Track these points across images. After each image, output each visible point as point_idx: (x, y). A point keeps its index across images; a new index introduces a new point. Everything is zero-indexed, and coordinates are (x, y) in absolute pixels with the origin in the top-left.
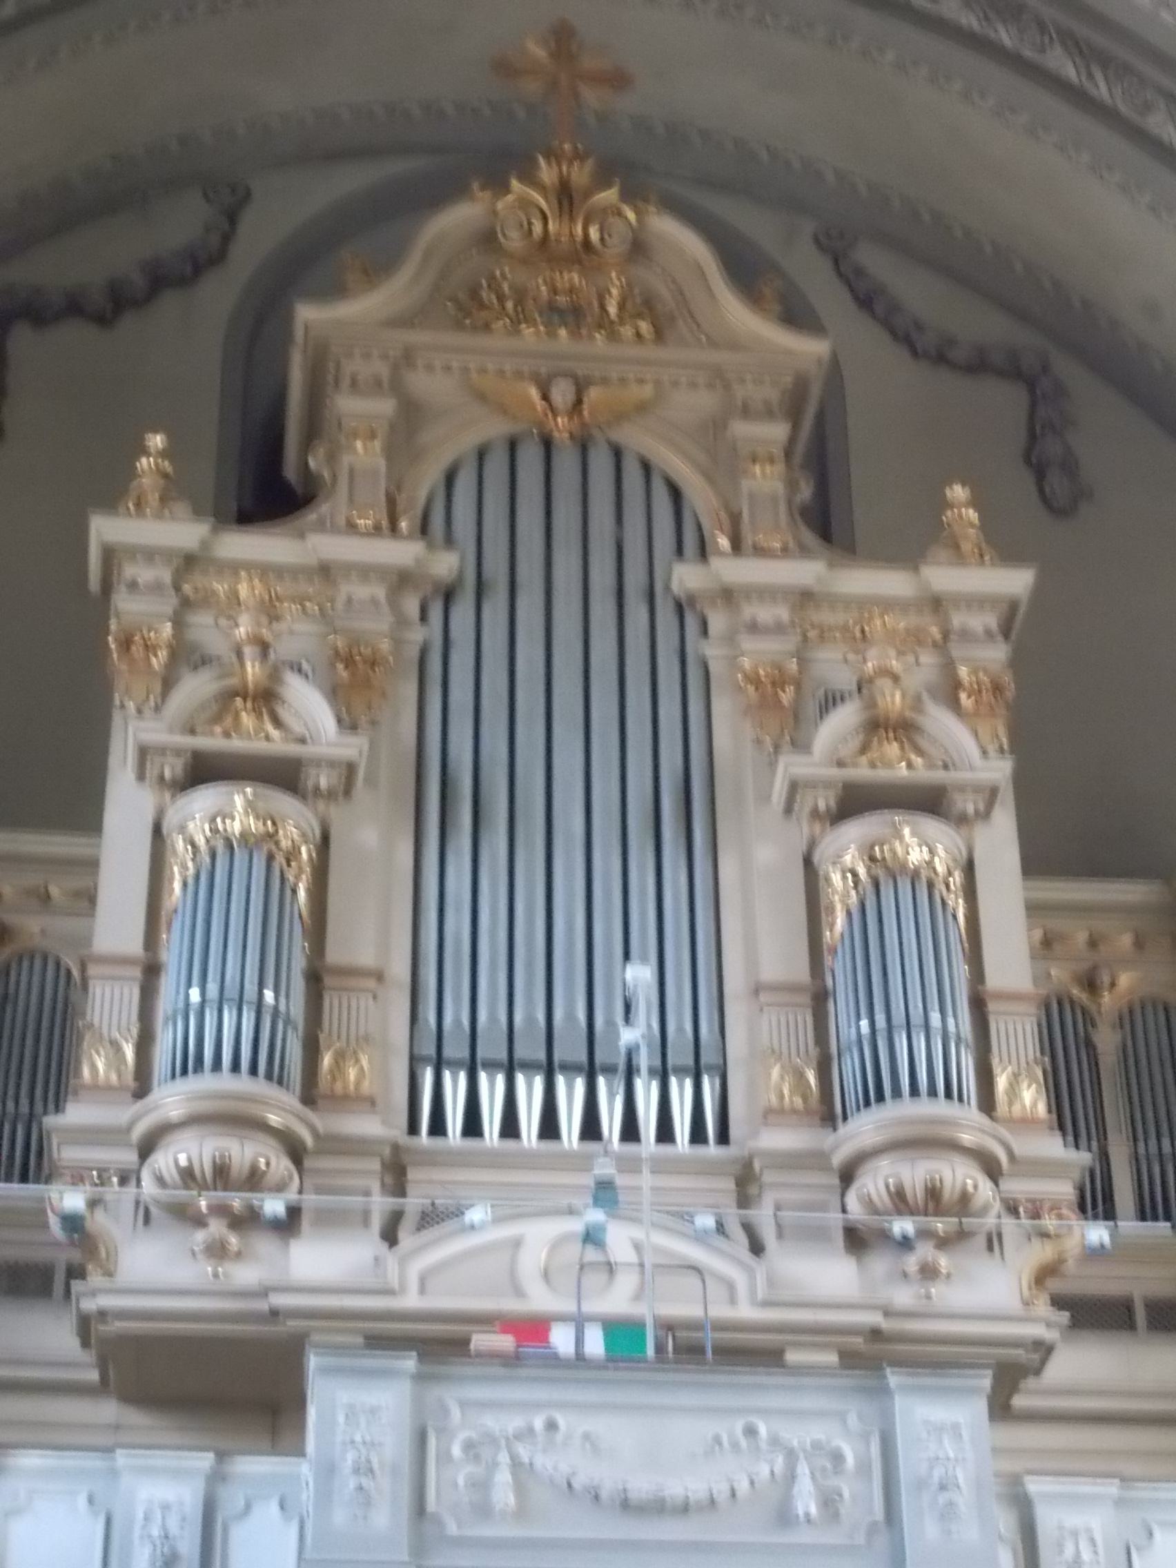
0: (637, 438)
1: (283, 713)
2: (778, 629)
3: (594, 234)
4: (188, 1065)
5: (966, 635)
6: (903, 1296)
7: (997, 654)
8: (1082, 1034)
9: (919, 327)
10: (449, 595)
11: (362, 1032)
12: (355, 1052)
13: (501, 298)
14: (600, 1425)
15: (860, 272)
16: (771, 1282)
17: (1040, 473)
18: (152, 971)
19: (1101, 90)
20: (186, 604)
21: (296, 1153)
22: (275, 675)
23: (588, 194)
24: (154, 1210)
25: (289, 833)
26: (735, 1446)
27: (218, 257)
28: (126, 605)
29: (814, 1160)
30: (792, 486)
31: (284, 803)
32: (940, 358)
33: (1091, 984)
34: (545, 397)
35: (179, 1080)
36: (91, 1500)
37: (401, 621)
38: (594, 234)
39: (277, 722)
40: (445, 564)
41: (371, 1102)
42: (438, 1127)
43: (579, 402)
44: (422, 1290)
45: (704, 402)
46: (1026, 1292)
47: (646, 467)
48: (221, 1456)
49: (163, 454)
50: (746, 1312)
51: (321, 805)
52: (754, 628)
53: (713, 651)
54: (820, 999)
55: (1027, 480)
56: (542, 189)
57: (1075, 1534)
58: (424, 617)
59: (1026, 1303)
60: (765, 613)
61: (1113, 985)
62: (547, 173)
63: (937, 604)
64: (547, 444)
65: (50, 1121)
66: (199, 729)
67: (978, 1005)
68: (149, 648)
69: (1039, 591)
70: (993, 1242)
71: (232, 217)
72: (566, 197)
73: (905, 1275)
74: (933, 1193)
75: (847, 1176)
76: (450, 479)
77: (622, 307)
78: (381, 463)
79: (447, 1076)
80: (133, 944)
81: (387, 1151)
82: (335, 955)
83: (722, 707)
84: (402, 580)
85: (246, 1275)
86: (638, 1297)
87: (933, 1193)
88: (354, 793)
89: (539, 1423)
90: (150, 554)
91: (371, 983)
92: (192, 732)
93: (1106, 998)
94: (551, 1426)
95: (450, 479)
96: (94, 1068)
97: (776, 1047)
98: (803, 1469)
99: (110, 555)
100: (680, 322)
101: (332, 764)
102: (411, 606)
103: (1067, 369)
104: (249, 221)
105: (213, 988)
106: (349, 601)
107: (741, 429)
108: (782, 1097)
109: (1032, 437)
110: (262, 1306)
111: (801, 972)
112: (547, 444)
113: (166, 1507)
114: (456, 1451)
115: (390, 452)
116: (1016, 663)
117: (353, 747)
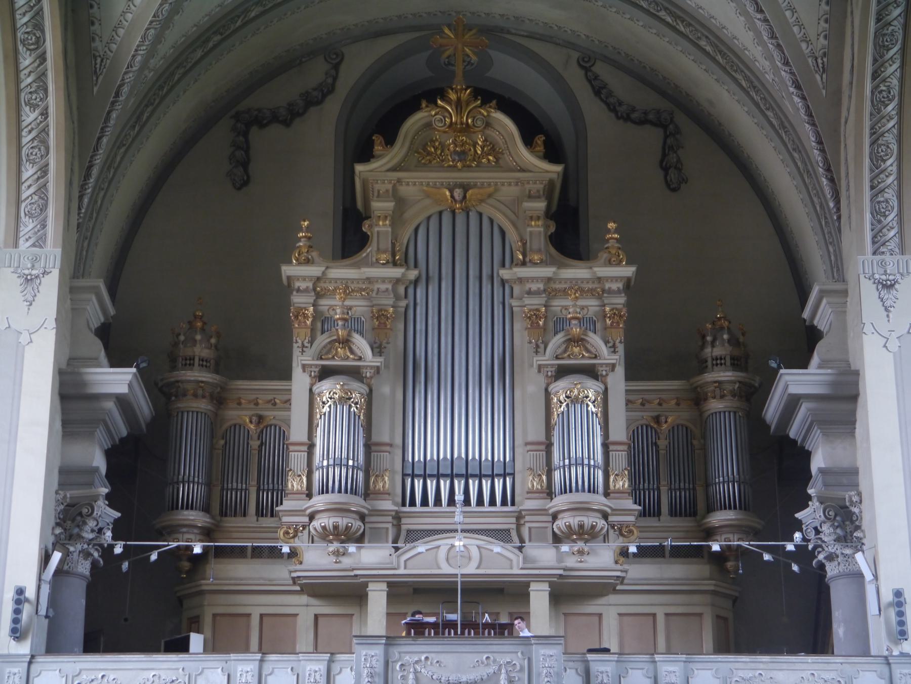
0: (486, 210)
1: (354, 347)
2: (538, 293)
3: (470, 121)
4: (324, 490)
5: (610, 291)
6: (571, 562)
7: (621, 300)
8: (654, 441)
9: (620, 104)
10: (416, 282)
11: (385, 468)
12: (383, 476)
13: (435, 149)
14: (441, 657)
15: (596, 77)
16: (525, 560)
17: (666, 170)
18: (311, 447)
19: (681, 28)
20: (318, 296)
21: (362, 517)
22: (349, 335)
23: (468, 104)
24: (315, 538)
25: (356, 396)
26: (483, 663)
27: (331, 90)
28: (298, 300)
29: (542, 511)
30: (547, 227)
31: (355, 385)
32: (627, 118)
33: (657, 419)
34: (452, 196)
35: (321, 495)
36: (292, 669)
37: (397, 298)
38: (470, 121)
39: (352, 352)
40: (413, 274)
41: (389, 494)
42: (413, 503)
43: (465, 197)
44: (405, 568)
45: (514, 191)
46: (616, 557)
47: (492, 221)
48: (332, 654)
49: (308, 229)
50: (516, 571)
51: (368, 381)
52: (529, 293)
53: (514, 303)
54: (549, 446)
55: (661, 174)
56: (449, 102)
57: (602, 673)
58: (406, 297)
59: (616, 562)
60: (534, 287)
61: (666, 422)
62: (453, 96)
63: (599, 279)
64: (453, 212)
65: (277, 509)
66: (323, 357)
67: (606, 446)
68: (306, 317)
69: (638, 272)
70: (606, 539)
71: (336, 67)
72: (459, 106)
73: (573, 554)
74: (581, 526)
75: (555, 517)
76: (416, 230)
77: (483, 148)
78: (390, 229)
79: (416, 481)
80: (304, 438)
81: (393, 513)
82: (375, 438)
83: (517, 326)
84: (397, 281)
85: (346, 562)
86: (478, 568)
87: (581, 526)
88: (381, 372)
89: (423, 658)
90: (304, 279)
91: (388, 448)
92: (321, 359)
93: (665, 426)
94: (427, 658)
95: (416, 230)
96: (293, 486)
97: (532, 467)
98: (503, 671)
99: (289, 278)
100: (506, 155)
101: (371, 367)
102: (401, 290)
103: (681, 119)
104: (343, 67)
105: (331, 462)
106: (378, 289)
107: (527, 205)
108: (533, 485)
109: (664, 155)
110: (352, 574)
111: (542, 437)
112: (453, 212)
113: (316, 672)
114: (398, 668)
115: (392, 225)
116: (628, 304)
117: (378, 361)
